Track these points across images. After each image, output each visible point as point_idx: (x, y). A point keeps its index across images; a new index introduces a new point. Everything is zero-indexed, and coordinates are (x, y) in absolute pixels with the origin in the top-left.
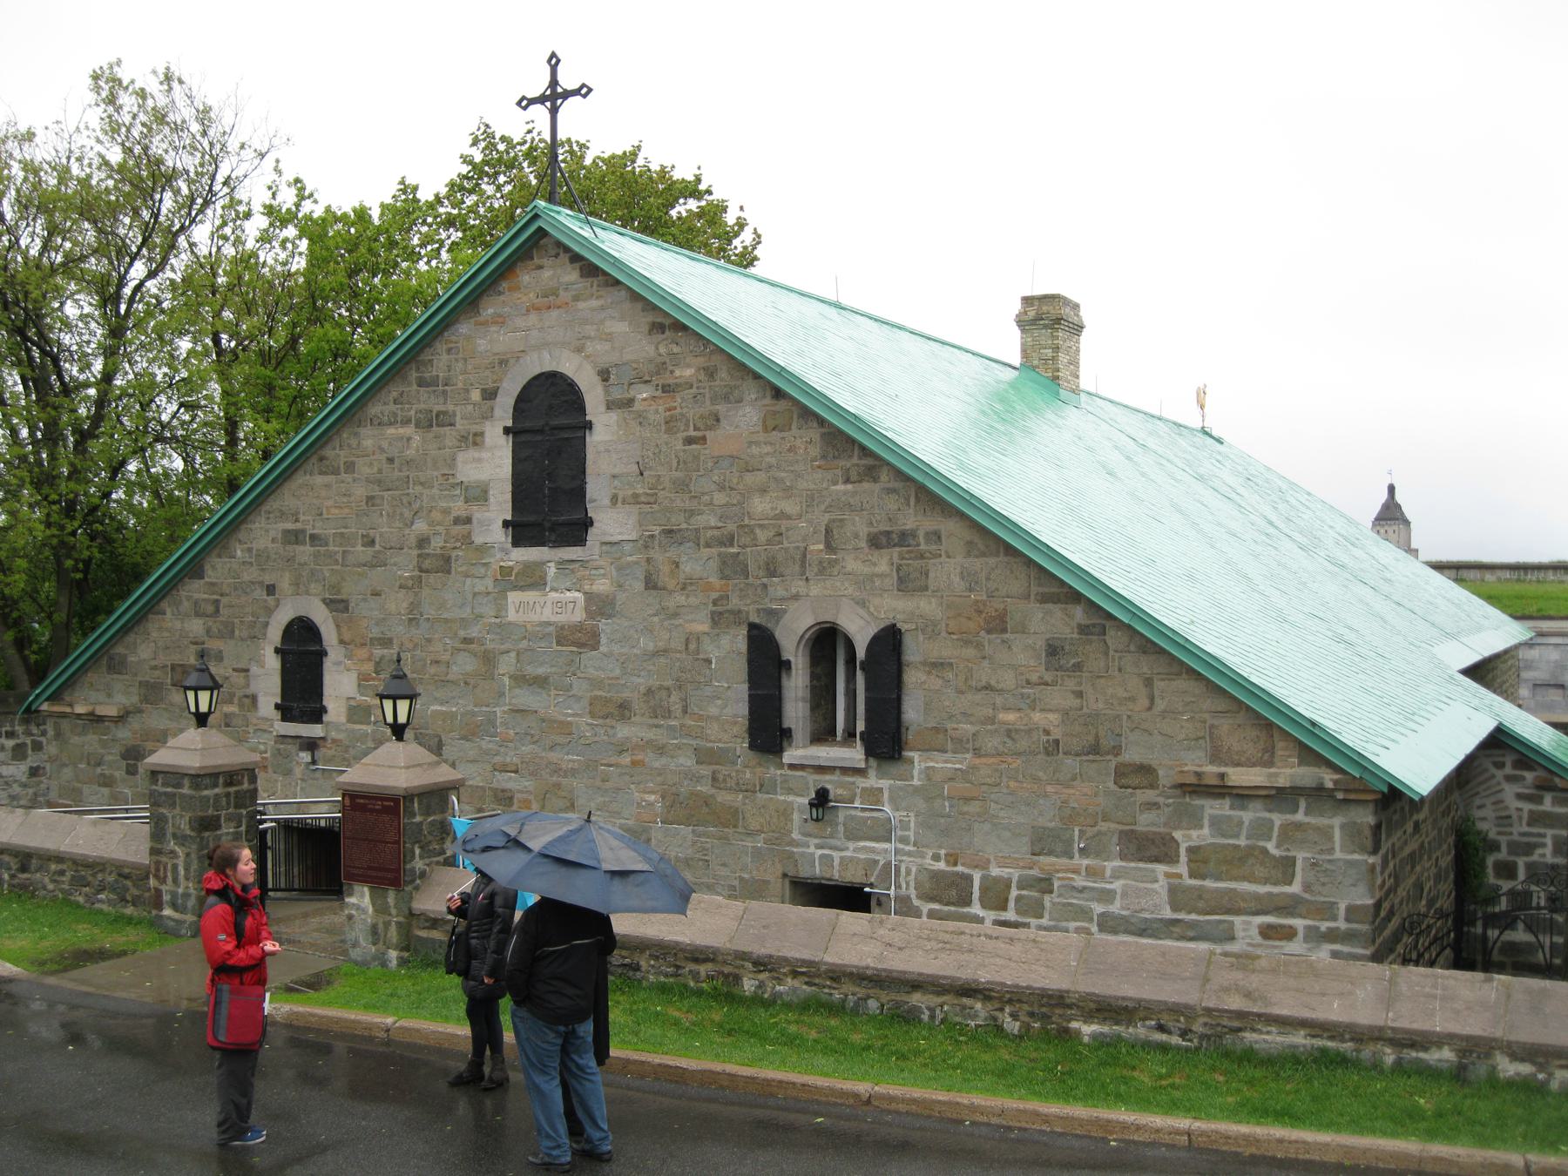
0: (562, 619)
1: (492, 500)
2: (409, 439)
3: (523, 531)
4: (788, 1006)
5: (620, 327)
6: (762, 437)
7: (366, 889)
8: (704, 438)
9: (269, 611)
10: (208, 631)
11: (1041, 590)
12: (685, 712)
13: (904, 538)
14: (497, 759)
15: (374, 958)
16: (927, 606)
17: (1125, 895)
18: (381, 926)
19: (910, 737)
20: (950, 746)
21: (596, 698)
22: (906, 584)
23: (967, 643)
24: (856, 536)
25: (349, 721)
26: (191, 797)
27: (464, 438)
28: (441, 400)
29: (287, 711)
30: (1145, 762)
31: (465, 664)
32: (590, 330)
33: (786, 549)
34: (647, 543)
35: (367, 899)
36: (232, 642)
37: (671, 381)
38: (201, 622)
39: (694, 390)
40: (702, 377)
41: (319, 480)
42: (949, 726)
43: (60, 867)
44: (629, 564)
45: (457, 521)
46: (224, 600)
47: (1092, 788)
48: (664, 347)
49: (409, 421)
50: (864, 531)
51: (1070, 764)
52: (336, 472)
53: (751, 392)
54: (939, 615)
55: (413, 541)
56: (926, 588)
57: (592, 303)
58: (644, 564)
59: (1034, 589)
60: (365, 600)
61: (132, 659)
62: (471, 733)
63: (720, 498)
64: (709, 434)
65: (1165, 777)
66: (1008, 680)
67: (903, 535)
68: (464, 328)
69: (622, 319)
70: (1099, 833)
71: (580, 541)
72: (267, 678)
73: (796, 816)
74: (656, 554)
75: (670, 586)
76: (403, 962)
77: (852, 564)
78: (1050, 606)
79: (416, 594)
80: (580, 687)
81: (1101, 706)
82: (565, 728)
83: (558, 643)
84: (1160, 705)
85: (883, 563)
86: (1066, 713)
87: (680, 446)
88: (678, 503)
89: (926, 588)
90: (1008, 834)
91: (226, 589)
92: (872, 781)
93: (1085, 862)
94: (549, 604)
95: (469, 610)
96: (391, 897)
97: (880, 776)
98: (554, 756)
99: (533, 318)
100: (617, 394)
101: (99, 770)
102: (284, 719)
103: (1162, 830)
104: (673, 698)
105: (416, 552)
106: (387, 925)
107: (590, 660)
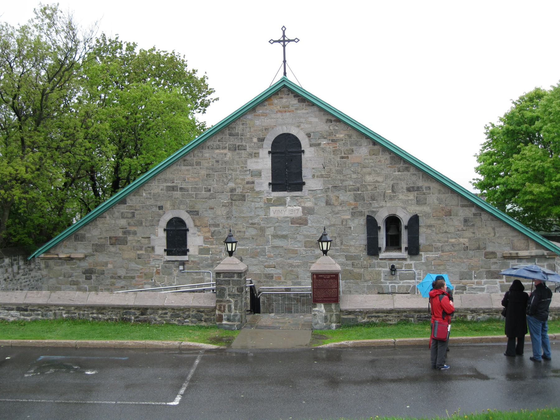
0: (293, 215)
1: (263, 175)
2: (225, 154)
3: (276, 186)
4: (482, 322)
5: (314, 120)
6: (369, 157)
7: (322, 305)
8: (348, 157)
9: (160, 216)
10: (129, 224)
11: (462, 203)
12: (342, 244)
13: (418, 189)
14: (266, 264)
15: (325, 327)
16: (426, 209)
17: (488, 289)
18: (329, 316)
19: (421, 247)
20: (434, 250)
21: (307, 241)
22: (419, 202)
23: (439, 219)
24: (402, 188)
25: (199, 254)
26: (238, 281)
27: (251, 155)
28: (240, 141)
29: (169, 252)
30: (493, 251)
31: (252, 232)
32: (303, 120)
33: (378, 192)
34: (327, 190)
35: (323, 308)
36: (141, 228)
37: (335, 138)
38: (125, 220)
39: (344, 142)
40: (347, 137)
41: (184, 168)
42: (434, 244)
43: (164, 311)
44: (319, 197)
45: (248, 183)
46: (136, 212)
47: (478, 259)
48: (332, 127)
49: (226, 148)
50: (405, 187)
51: (471, 253)
52: (192, 165)
53: (364, 142)
54: (430, 211)
55: (228, 189)
56: (426, 203)
57: (304, 111)
58: (325, 197)
59: (460, 203)
60: (206, 211)
61: (88, 235)
62: (254, 255)
63: (354, 176)
64: (349, 156)
65: (499, 255)
66: (452, 229)
67: (418, 188)
68: (249, 117)
69: (316, 117)
70: (480, 272)
71: (301, 190)
72: (160, 240)
73: (382, 274)
74: (330, 194)
75: (336, 204)
76: (337, 327)
77: (401, 197)
78: (464, 208)
79: (230, 208)
80: (300, 238)
81: (480, 236)
82: (295, 252)
83: (291, 224)
84: (497, 235)
85: (411, 196)
86: (470, 239)
87: (339, 159)
88: (339, 177)
89: (426, 203)
90: (452, 274)
91: (138, 208)
92: (408, 262)
93: (476, 280)
94: (288, 210)
95: (253, 213)
96: (333, 306)
97: (411, 260)
98: (290, 261)
99: (279, 115)
100: (313, 142)
101: (70, 279)
102: (168, 255)
103: (498, 270)
104: (337, 240)
105: (230, 194)
106: (331, 316)
107: (304, 230)
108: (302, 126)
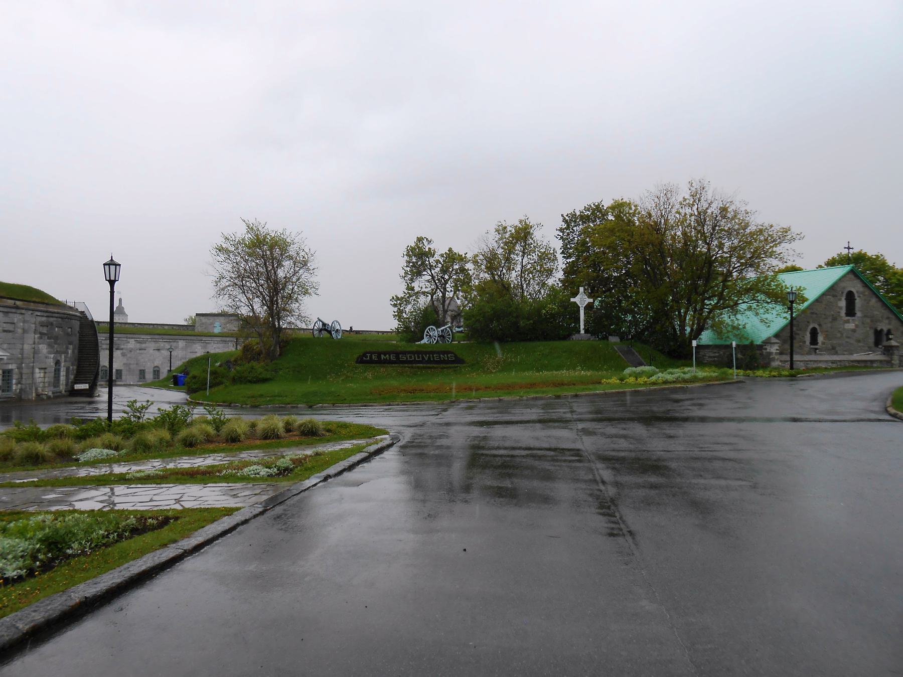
22: (890, 324)
31: (839, 335)
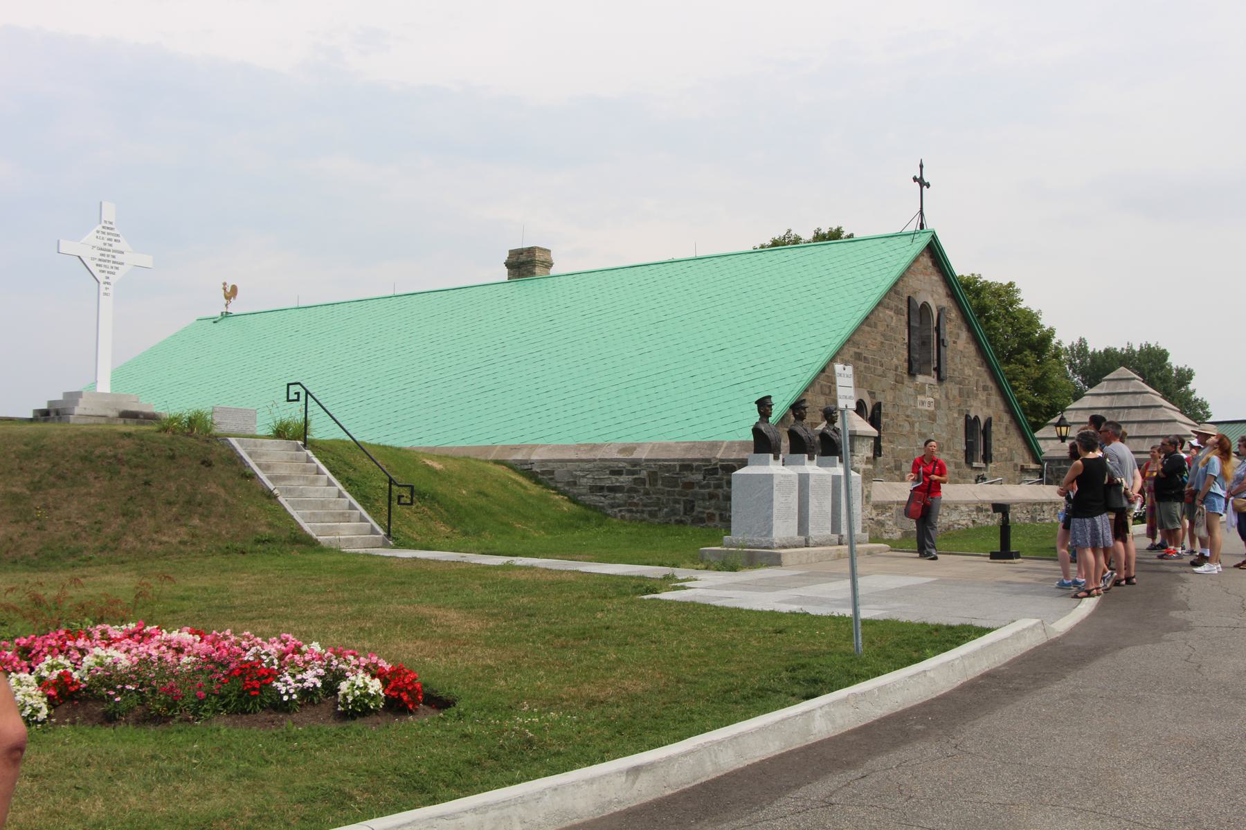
31: (907, 427)
66: (1000, 437)
99: (921, 277)
108: (936, 296)
